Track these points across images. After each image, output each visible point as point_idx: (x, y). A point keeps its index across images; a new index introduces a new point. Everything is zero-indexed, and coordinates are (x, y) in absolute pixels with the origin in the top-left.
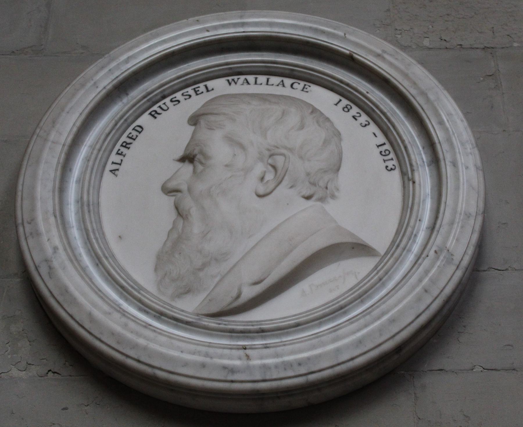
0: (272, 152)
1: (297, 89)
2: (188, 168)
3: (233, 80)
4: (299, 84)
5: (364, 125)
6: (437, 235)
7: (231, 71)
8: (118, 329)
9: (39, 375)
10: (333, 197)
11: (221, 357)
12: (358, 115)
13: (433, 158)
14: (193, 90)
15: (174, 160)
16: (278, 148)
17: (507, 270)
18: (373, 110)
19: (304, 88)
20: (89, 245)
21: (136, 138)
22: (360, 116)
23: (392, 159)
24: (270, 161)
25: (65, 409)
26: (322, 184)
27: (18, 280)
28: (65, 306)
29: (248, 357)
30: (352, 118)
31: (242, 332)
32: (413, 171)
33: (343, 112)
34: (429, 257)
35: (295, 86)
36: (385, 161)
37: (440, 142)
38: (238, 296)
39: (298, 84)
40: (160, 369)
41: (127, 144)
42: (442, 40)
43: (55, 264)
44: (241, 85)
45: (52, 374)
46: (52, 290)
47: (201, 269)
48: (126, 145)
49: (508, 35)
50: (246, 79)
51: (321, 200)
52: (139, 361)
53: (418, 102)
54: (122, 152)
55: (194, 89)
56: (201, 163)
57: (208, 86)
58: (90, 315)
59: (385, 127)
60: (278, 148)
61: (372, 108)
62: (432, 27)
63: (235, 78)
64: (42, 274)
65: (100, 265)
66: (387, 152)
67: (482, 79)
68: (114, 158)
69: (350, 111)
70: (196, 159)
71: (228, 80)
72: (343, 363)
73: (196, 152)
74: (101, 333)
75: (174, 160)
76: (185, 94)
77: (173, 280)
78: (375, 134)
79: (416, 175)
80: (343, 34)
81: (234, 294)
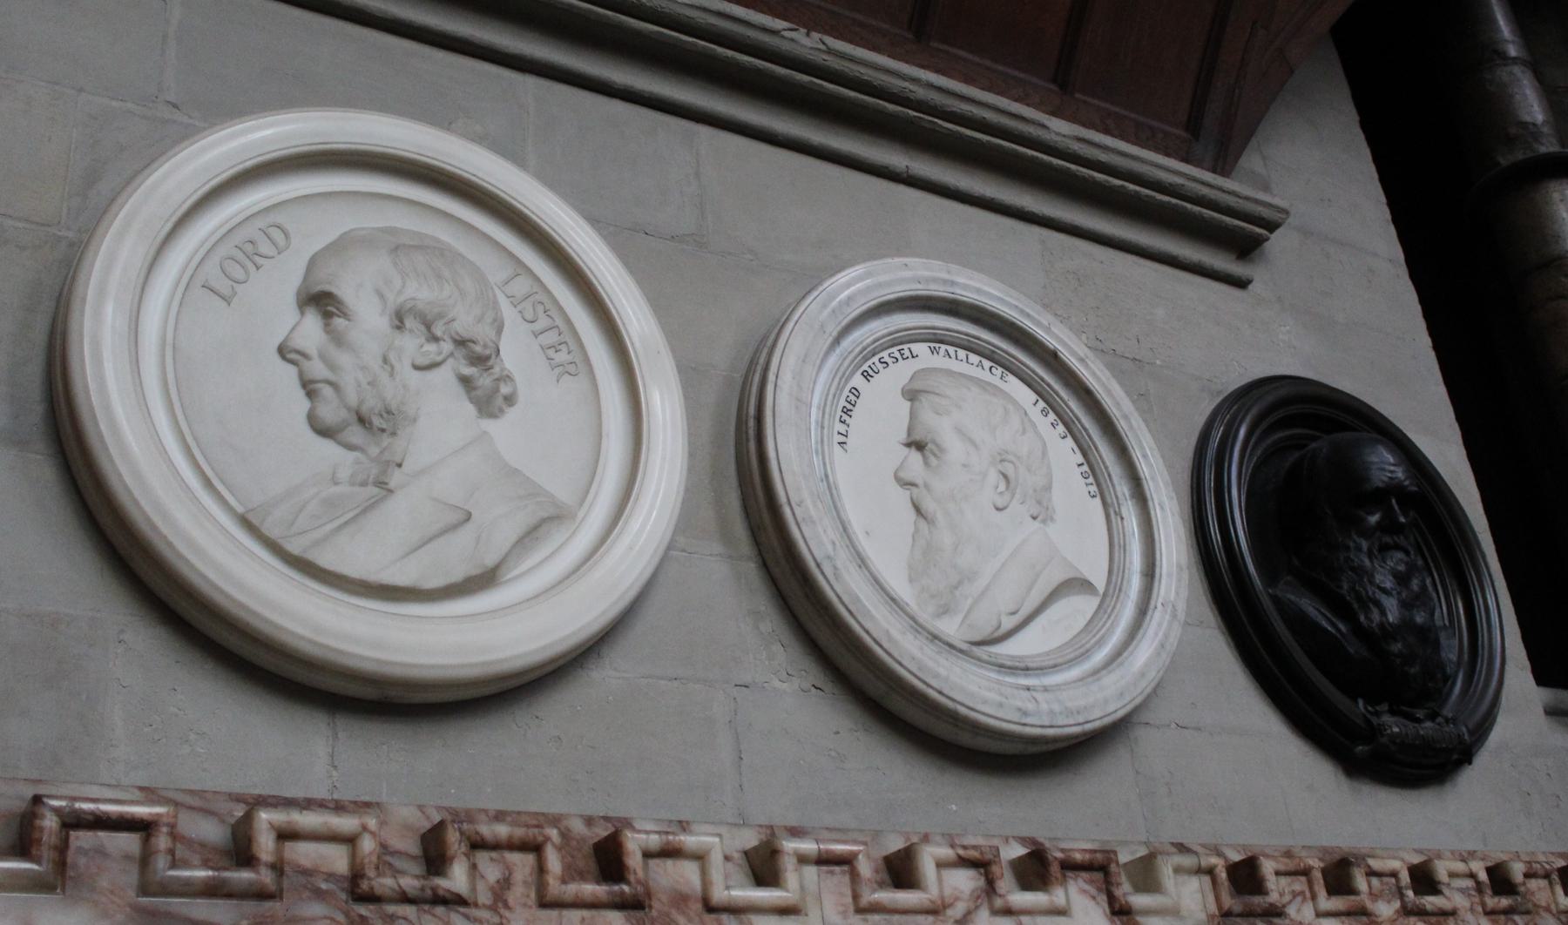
0: (1003, 457)
2: (915, 456)
3: (934, 348)
8: (918, 654)
14: (898, 353)
18: (1073, 421)
23: (1092, 484)
25: (838, 733)
31: (1010, 668)
38: (999, 627)
41: (848, 410)
43: (839, 564)
47: (956, 588)
48: (846, 411)
50: (947, 351)
51: (1044, 522)
52: (940, 693)
53: (1121, 425)
55: (899, 350)
56: (935, 455)
60: (1007, 452)
63: (937, 345)
71: (930, 347)
76: (892, 355)
77: (933, 596)
81: (995, 623)
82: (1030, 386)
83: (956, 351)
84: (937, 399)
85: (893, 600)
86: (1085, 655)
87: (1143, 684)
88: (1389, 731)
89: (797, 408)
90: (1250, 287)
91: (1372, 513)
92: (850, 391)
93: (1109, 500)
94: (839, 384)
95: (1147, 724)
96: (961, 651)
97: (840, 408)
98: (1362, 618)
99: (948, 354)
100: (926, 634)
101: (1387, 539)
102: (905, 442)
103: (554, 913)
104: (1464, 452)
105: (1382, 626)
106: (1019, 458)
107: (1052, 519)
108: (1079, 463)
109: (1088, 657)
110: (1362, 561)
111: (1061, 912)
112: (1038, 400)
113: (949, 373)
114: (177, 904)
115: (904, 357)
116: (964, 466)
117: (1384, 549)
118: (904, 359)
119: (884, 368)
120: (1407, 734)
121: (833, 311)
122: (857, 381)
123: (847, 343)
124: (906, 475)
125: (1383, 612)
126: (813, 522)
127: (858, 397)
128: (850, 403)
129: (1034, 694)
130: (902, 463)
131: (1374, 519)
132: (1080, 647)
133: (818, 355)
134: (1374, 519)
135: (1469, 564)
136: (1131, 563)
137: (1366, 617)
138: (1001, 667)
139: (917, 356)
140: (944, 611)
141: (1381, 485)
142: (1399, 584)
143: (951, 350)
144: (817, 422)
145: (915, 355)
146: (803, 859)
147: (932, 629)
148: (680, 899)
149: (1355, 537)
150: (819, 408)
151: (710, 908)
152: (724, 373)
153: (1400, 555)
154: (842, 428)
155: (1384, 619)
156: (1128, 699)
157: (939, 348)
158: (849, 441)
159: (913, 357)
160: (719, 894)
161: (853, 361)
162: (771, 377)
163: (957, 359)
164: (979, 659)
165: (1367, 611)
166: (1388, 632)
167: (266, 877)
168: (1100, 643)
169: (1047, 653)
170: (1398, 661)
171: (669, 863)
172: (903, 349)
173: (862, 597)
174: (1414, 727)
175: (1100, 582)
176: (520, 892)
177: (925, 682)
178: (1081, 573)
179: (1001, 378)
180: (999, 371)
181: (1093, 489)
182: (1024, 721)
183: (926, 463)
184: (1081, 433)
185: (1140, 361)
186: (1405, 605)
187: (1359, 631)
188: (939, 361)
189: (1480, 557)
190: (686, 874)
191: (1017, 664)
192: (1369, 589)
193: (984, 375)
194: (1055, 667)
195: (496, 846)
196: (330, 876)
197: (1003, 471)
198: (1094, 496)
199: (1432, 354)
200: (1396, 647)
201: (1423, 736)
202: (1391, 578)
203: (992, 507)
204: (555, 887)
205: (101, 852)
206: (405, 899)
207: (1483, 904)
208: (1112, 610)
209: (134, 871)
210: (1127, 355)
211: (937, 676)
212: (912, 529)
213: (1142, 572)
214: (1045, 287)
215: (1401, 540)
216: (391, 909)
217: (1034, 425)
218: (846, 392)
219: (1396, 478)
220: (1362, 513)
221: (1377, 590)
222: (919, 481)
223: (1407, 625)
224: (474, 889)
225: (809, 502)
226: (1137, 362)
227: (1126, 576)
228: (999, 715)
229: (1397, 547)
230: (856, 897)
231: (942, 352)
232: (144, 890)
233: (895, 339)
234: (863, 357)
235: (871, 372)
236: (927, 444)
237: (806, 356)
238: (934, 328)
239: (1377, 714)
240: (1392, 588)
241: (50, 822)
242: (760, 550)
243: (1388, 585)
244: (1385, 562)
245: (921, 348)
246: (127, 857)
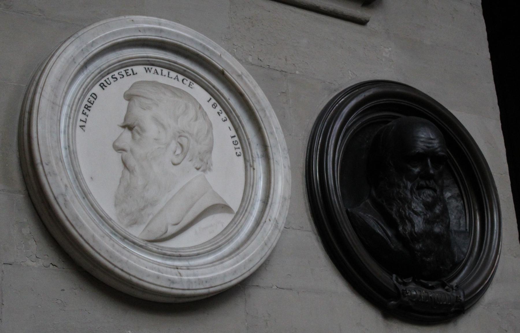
0: (181, 134)
1: (186, 84)
2: (127, 134)
3: (148, 68)
4: (187, 81)
5: (224, 120)
6: (270, 209)
7: (148, 62)
8: (111, 248)
9: (45, 265)
10: (210, 169)
11: (167, 273)
12: (220, 112)
13: (263, 154)
14: (124, 72)
15: (118, 125)
16: (184, 132)
17: (289, 228)
18: (231, 112)
19: (190, 84)
20: (77, 182)
21: (93, 103)
22: (222, 113)
23: (239, 148)
24: (179, 140)
25: (63, 290)
26: (205, 160)
27: (22, 196)
28: (77, 228)
29: (181, 275)
30: (217, 114)
31: (169, 255)
32: (253, 161)
33: (211, 106)
34: (266, 223)
35: (185, 81)
36: (235, 149)
37: (271, 146)
38: (166, 232)
39: (186, 80)
40: (134, 277)
41: (88, 107)
42: (259, 59)
43: (68, 198)
44: (153, 74)
45: (52, 266)
46: (67, 215)
47: (142, 209)
48: (87, 107)
49: (294, 64)
50: (156, 70)
51: (204, 171)
52: (122, 270)
53: (259, 115)
54: (86, 113)
55: (125, 71)
56: (139, 133)
57: (134, 70)
58: (93, 236)
59: (237, 126)
60: (184, 132)
61: (230, 110)
62: (254, 47)
63: (150, 67)
64: (60, 203)
65: (86, 198)
66: (237, 143)
67: (279, 94)
68: (81, 116)
69: (216, 107)
70: (134, 129)
71: (145, 68)
72: (226, 283)
73: (135, 124)
74: (100, 250)
75: (118, 125)
76: (120, 73)
77: (127, 215)
78: (230, 128)
79: (255, 164)
80: (220, 54)
81: (163, 230)
82: (206, 90)
83: (162, 70)
84: (143, 100)
85: (101, 217)
86: (219, 248)
87: (251, 265)
88: (409, 294)
89: (52, 108)
90: (368, 24)
91: (416, 167)
92: (91, 96)
93: (247, 158)
94: (83, 92)
95: (258, 286)
96: (141, 246)
97: (83, 105)
98: (401, 228)
99: (157, 72)
100: (120, 236)
101: (422, 183)
102: (121, 125)
104: (500, 124)
105: (411, 233)
106: (190, 134)
107: (210, 169)
108: (232, 136)
109: (221, 249)
110: (406, 194)
112: (211, 99)
113: (155, 84)
115: (128, 74)
116: (156, 139)
117: (420, 188)
118: (127, 76)
119: (114, 81)
120: (420, 296)
121: (82, 50)
122: (97, 89)
123: (91, 68)
124: (121, 145)
125: (413, 226)
126: (55, 175)
127: (95, 99)
128: (90, 102)
129: (180, 271)
130: (118, 138)
131: (417, 170)
132: (216, 244)
133: (70, 76)
134: (417, 170)
135: (486, 195)
136: (256, 195)
137: (403, 228)
138: (164, 255)
139: (136, 74)
140: (134, 223)
141: (421, 151)
142: (426, 209)
143: (159, 69)
144: (67, 114)
145: (135, 73)
147: (124, 233)
149: (404, 180)
150: (69, 106)
152: (16, 84)
153: (429, 192)
154: (83, 117)
155: (413, 230)
156: (239, 274)
157: (151, 68)
158: (87, 125)
159: (134, 74)
161: (93, 79)
162: (39, 90)
163: (162, 74)
164: (150, 250)
165: (404, 224)
166: (415, 238)
168: (228, 242)
169: (195, 247)
170: (419, 254)
172: (128, 70)
173: (80, 217)
174: (426, 292)
175: (235, 206)
177: (113, 265)
178: (225, 202)
179: (189, 86)
180: (188, 82)
181: (240, 151)
182: (172, 286)
183: (133, 137)
184: (235, 118)
185: (286, 72)
186: (427, 221)
187: (399, 236)
188: (150, 77)
189: (493, 190)
191: (174, 253)
192: (407, 211)
193: (178, 85)
194: (198, 255)
197: (181, 143)
198: (239, 155)
199: (489, 63)
200: (419, 246)
201: (431, 297)
202: (422, 206)
203: (171, 163)
208: (239, 223)
210: (276, 69)
211: (121, 261)
212: (120, 176)
213: (261, 200)
214: (229, 28)
215: (432, 183)
217: (205, 115)
218: (88, 96)
219: (433, 147)
220: (409, 166)
221: (411, 212)
222: (127, 148)
223: (428, 234)
225: (54, 162)
226: (284, 73)
227: (251, 202)
228: (158, 283)
229: (428, 188)
231: (153, 71)
233: (122, 64)
234: (101, 76)
235: (105, 84)
236: (134, 127)
237: (61, 77)
238: (147, 57)
239: (405, 284)
240: (421, 212)
242: (27, 186)
243: (419, 209)
244: (419, 196)
245: (140, 69)
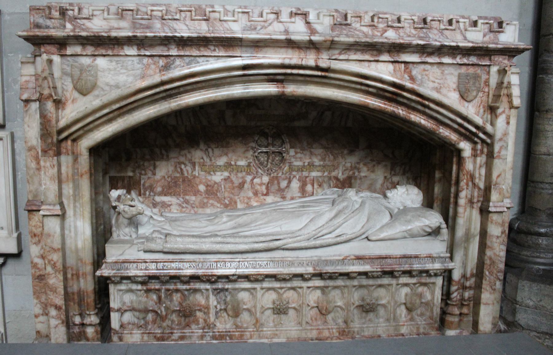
103: (193, 21)
111: (294, 23)
114: (137, 21)
146: (239, 12)
148: (215, 19)
151: (221, 21)
160: (222, 18)
167: (149, 17)
171: (214, 13)
176: (188, 18)
190: (216, 15)
195: (184, 11)
196: (159, 17)
204: (194, 18)
205: (127, 14)
206: (170, 19)
207: (414, 26)
209: (132, 16)
216: (168, 21)
224: (180, 18)
230: (249, 19)
232: (133, 19)
241: (120, 10)
246: (130, 15)
